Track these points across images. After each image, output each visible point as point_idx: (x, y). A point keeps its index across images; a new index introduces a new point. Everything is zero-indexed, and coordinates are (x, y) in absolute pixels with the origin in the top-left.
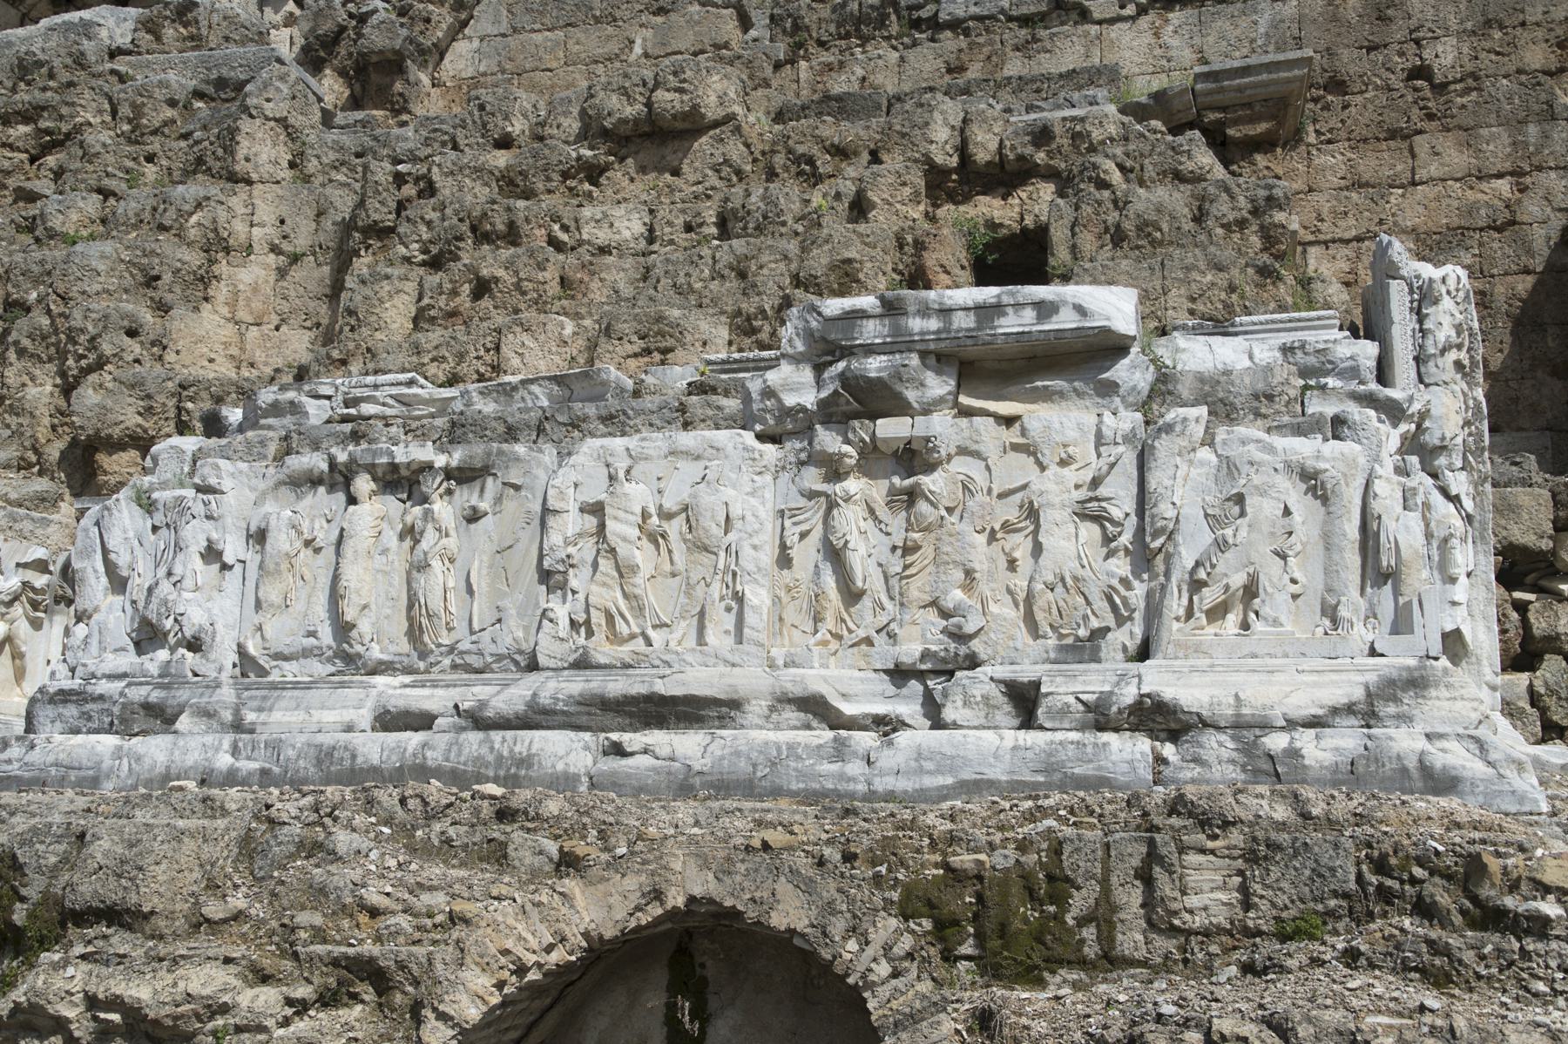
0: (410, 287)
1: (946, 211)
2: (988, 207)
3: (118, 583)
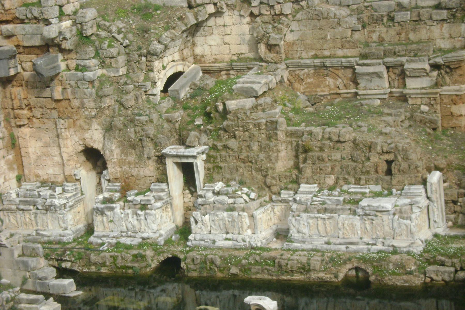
0: (310, 167)
1: (381, 157)
2: (387, 157)
3: (294, 227)
